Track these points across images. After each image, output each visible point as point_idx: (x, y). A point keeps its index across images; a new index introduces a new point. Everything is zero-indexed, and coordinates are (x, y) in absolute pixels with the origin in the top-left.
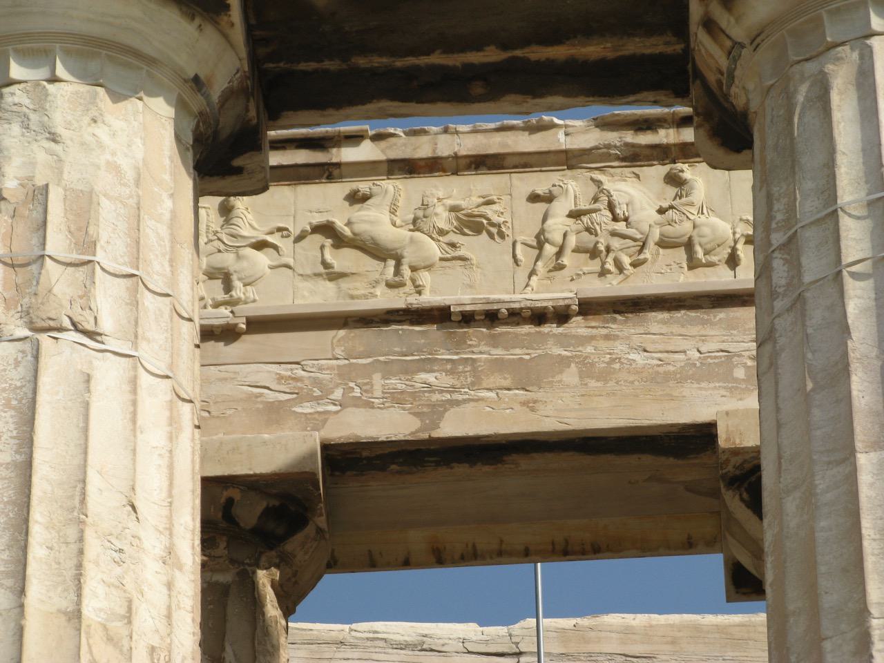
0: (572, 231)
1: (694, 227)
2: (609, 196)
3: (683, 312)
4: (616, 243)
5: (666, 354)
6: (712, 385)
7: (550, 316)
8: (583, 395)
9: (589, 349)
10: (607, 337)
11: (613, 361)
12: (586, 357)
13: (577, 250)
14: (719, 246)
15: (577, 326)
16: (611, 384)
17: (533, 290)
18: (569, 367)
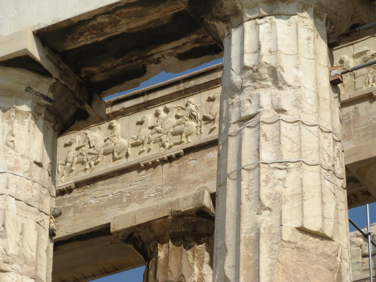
0: (75, 156)
1: (115, 144)
2: (89, 139)
3: (109, 179)
4: (90, 157)
5: (102, 198)
6: (115, 206)
7: (66, 191)
8: (74, 220)
9: (78, 201)
10: (84, 195)
11: (85, 204)
12: (76, 205)
13: (78, 163)
14: (122, 150)
15: (75, 193)
16: (84, 213)
17: (62, 182)
18: (71, 210)
